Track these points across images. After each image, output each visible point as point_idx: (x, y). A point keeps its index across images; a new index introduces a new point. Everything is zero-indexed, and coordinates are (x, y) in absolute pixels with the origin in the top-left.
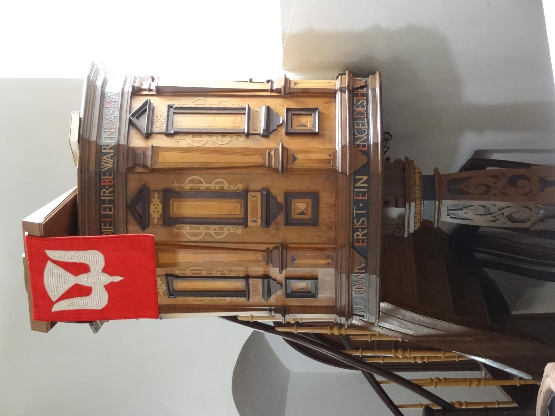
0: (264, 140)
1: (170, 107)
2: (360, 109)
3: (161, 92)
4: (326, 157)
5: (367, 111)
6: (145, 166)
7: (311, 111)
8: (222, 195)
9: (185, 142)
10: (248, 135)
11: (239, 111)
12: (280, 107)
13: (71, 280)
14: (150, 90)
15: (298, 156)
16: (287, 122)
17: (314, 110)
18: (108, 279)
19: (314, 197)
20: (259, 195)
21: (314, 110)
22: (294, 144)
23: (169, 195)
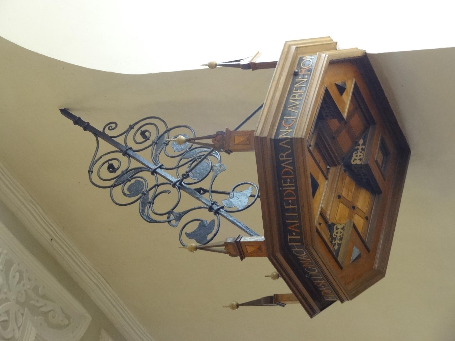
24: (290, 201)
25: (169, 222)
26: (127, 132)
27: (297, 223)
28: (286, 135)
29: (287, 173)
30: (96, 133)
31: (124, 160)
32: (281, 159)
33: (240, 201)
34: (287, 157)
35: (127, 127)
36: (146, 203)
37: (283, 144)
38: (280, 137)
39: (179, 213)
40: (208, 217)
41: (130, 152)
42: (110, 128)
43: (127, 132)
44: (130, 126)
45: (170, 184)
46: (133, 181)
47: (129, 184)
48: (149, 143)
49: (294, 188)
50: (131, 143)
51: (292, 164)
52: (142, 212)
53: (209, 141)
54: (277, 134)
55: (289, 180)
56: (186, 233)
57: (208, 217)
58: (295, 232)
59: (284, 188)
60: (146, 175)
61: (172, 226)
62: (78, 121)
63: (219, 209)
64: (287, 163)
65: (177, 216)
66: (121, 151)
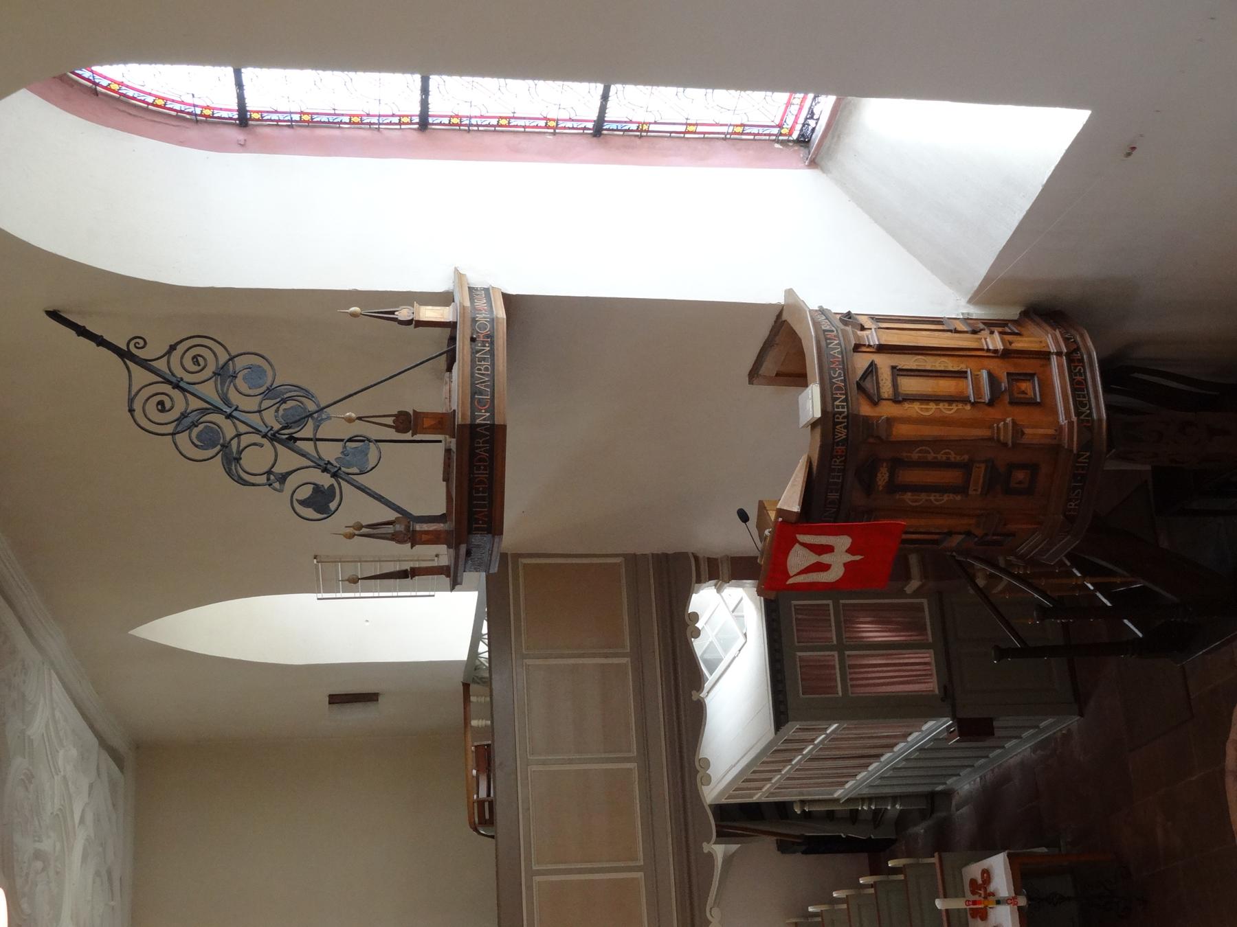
0: (990, 410)
1: (893, 368)
2: (1078, 378)
3: (882, 349)
4: (1051, 431)
5: (1085, 380)
6: (879, 438)
7: (1029, 377)
8: (948, 465)
9: (915, 409)
10: (973, 404)
11: (961, 375)
12: (1002, 369)
13: (813, 558)
14: (869, 346)
15: (1027, 431)
16: (1010, 390)
17: (1032, 375)
18: (849, 558)
19: (1033, 468)
20: (983, 466)
21: (1032, 375)
22: (1021, 415)
23: (897, 464)
30: (124, 355)
31: (176, 394)
35: (168, 348)
36: (231, 461)
38: (478, 421)
40: (326, 480)
41: (182, 384)
46: (201, 427)
47: (195, 431)
48: (208, 373)
50: (179, 372)
51: (491, 451)
52: (229, 473)
53: (390, 421)
54: (473, 417)
57: (326, 480)
61: (275, 489)
62: (82, 332)
66: (169, 382)
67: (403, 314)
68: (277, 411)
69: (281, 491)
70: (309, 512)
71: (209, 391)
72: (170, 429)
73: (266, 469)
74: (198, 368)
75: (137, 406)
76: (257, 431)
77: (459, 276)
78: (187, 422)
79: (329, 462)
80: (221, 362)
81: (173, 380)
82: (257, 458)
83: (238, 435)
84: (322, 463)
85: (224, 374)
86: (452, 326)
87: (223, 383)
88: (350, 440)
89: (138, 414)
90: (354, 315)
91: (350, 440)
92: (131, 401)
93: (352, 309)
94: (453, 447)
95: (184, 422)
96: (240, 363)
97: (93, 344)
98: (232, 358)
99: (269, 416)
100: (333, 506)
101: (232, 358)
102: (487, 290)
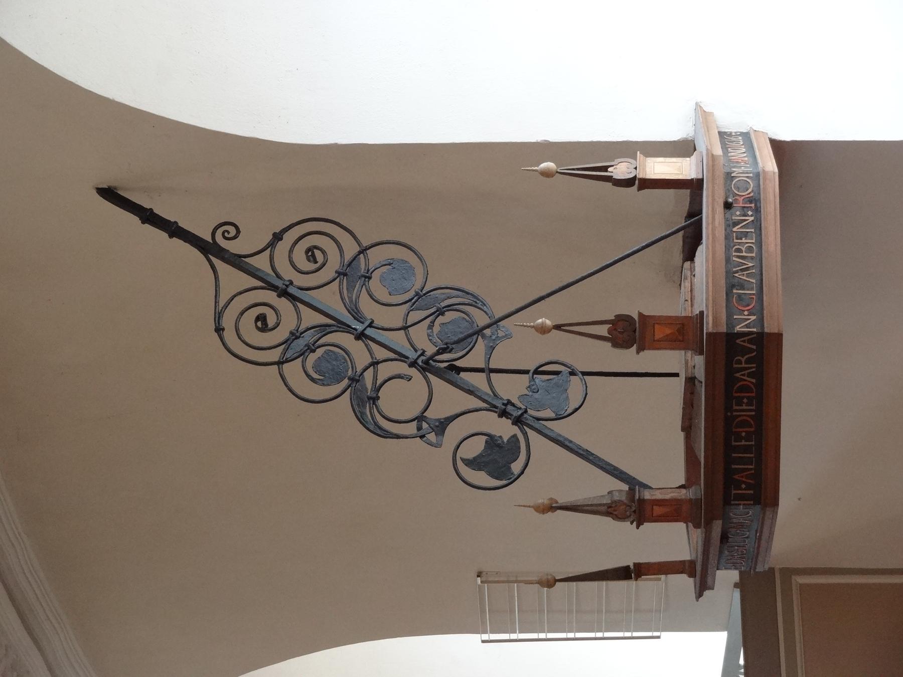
24: (743, 434)
25: (422, 437)
26: (272, 245)
27: (751, 469)
28: (747, 326)
29: (745, 389)
31: (283, 304)
32: (735, 366)
33: (554, 398)
34: (746, 363)
37: (744, 341)
38: (738, 329)
39: (439, 420)
40: (504, 429)
41: (291, 290)
42: (226, 234)
43: (272, 245)
44: (274, 234)
45: (405, 362)
46: (320, 352)
47: (312, 358)
49: (753, 413)
50: (288, 273)
53: (603, 330)
54: (730, 322)
55: (745, 400)
56: (463, 460)
58: (744, 482)
59: (735, 413)
60: (345, 339)
61: (430, 444)
62: (149, 217)
63: (522, 414)
64: (746, 372)
65: (437, 426)
66: (273, 288)
67: (621, 170)
68: (431, 327)
69: (438, 445)
70: (481, 478)
71: (331, 299)
72: (275, 355)
73: (416, 412)
74: (313, 267)
75: (228, 321)
76: (402, 357)
77: (703, 116)
78: (300, 344)
79: (509, 402)
80: (348, 257)
81: (279, 283)
82: (403, 397)
83: (375, 364)
84: (499, 404)
85: (351, 273)
86: (694, 186)
87: (350, 288)
88: (537, 372)
89: (230, 335)
90: (547, 174)
91: (537, 372)
92: (218, 316)
93: (544, 165)
94: (700, 374)
95: (296, 346)
96: (376, 256)
97: (165, 235)
98: (363, 251)
99: (419, 335)
100: (516, 467)
101: (363, 251)
102: (746, 136)
